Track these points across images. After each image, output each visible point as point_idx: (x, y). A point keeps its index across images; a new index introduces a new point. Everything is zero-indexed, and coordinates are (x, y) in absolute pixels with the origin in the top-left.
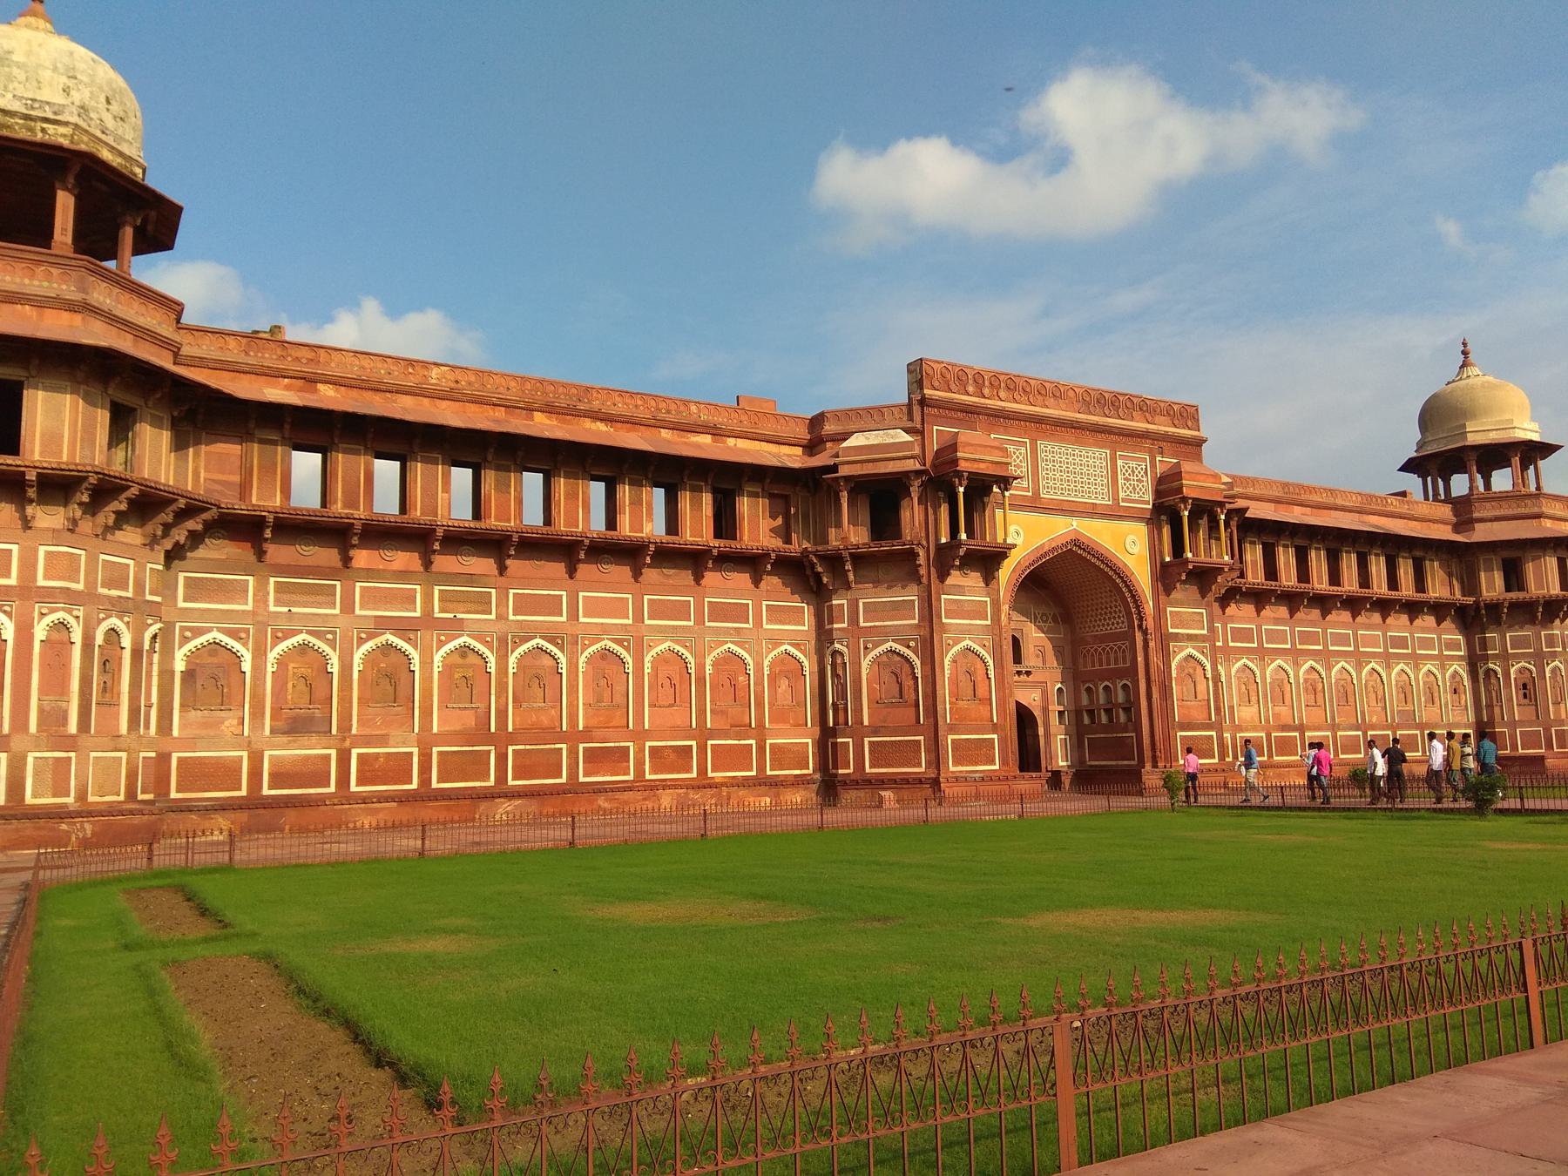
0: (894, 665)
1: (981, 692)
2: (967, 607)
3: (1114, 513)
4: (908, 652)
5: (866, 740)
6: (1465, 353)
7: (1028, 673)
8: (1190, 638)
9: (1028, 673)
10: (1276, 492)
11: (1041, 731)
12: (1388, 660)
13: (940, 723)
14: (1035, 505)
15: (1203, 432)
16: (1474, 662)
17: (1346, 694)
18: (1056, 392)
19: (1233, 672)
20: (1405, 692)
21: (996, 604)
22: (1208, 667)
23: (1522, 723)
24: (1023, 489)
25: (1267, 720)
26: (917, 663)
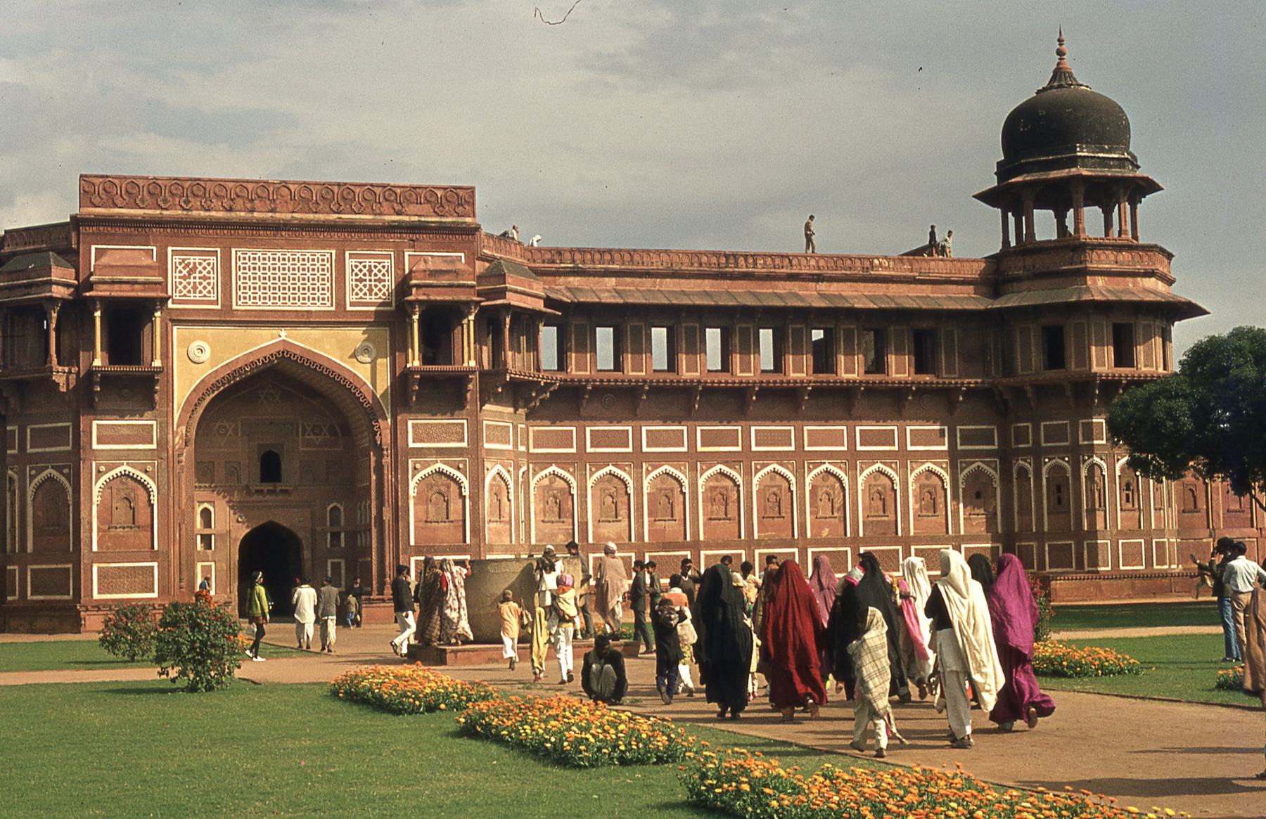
0: (50, 490)
1: (142, 518)
2: (125, 432)
3: (338, 320)
4: (63, 479)
5: (30, 567)
6: (1060, 53)
7: (286, 491)
8: (440, 452)
9: (285, 492)
10: (712, 265)
11: (306, 554)
12: (852, 459)
13: (84, 550)
14: (226, 318)
15: (478, 220)
16: (1005, 457)
17: (777, 502)
18: (265, 191)
19: (590, 483)
20: (883, 496)
21: (164, 427)
22: (466, 483)
23: (1052, 535)
24: (211, 303)
25: (640, 536)
26: (70, 490)
